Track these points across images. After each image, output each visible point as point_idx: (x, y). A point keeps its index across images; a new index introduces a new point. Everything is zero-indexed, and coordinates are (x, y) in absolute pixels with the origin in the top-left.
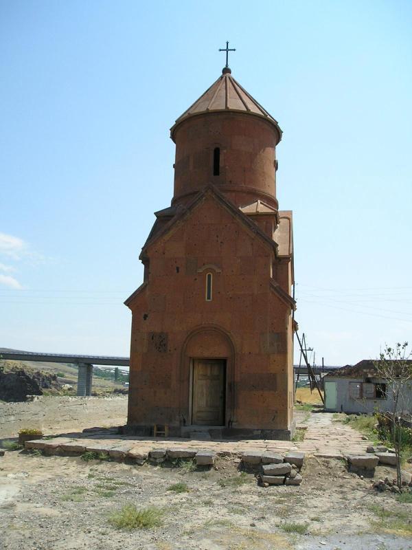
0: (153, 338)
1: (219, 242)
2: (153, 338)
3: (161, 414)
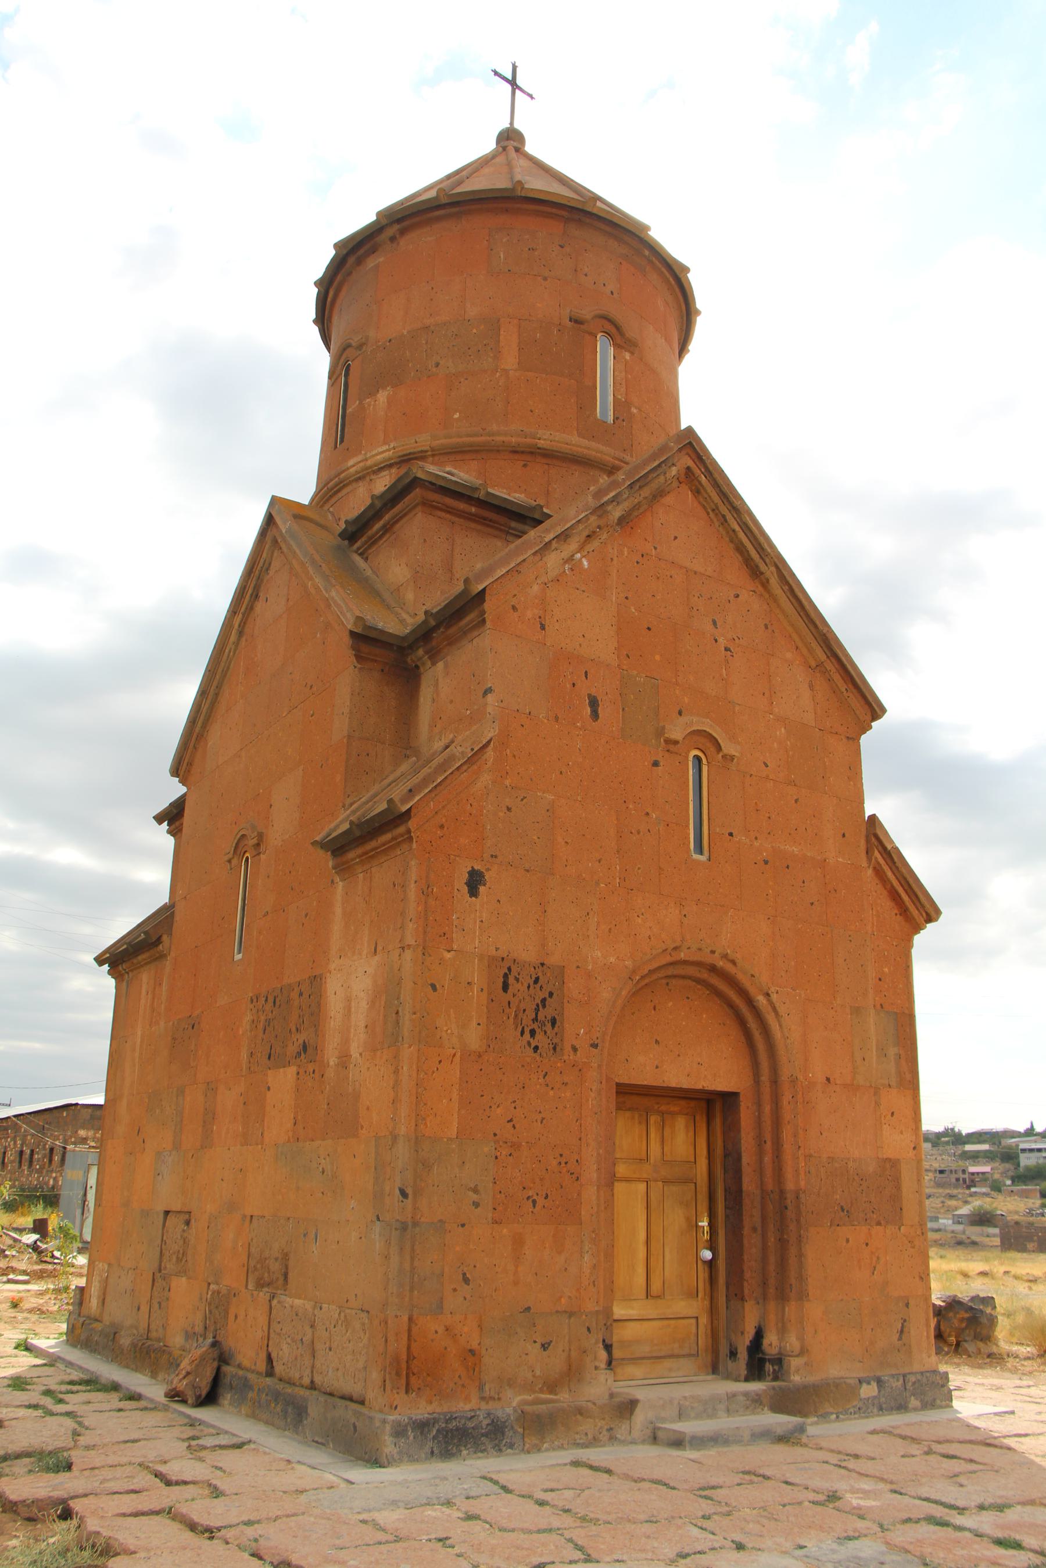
0: (505, 987)
2: (505, 987)
3: (544, 1347)
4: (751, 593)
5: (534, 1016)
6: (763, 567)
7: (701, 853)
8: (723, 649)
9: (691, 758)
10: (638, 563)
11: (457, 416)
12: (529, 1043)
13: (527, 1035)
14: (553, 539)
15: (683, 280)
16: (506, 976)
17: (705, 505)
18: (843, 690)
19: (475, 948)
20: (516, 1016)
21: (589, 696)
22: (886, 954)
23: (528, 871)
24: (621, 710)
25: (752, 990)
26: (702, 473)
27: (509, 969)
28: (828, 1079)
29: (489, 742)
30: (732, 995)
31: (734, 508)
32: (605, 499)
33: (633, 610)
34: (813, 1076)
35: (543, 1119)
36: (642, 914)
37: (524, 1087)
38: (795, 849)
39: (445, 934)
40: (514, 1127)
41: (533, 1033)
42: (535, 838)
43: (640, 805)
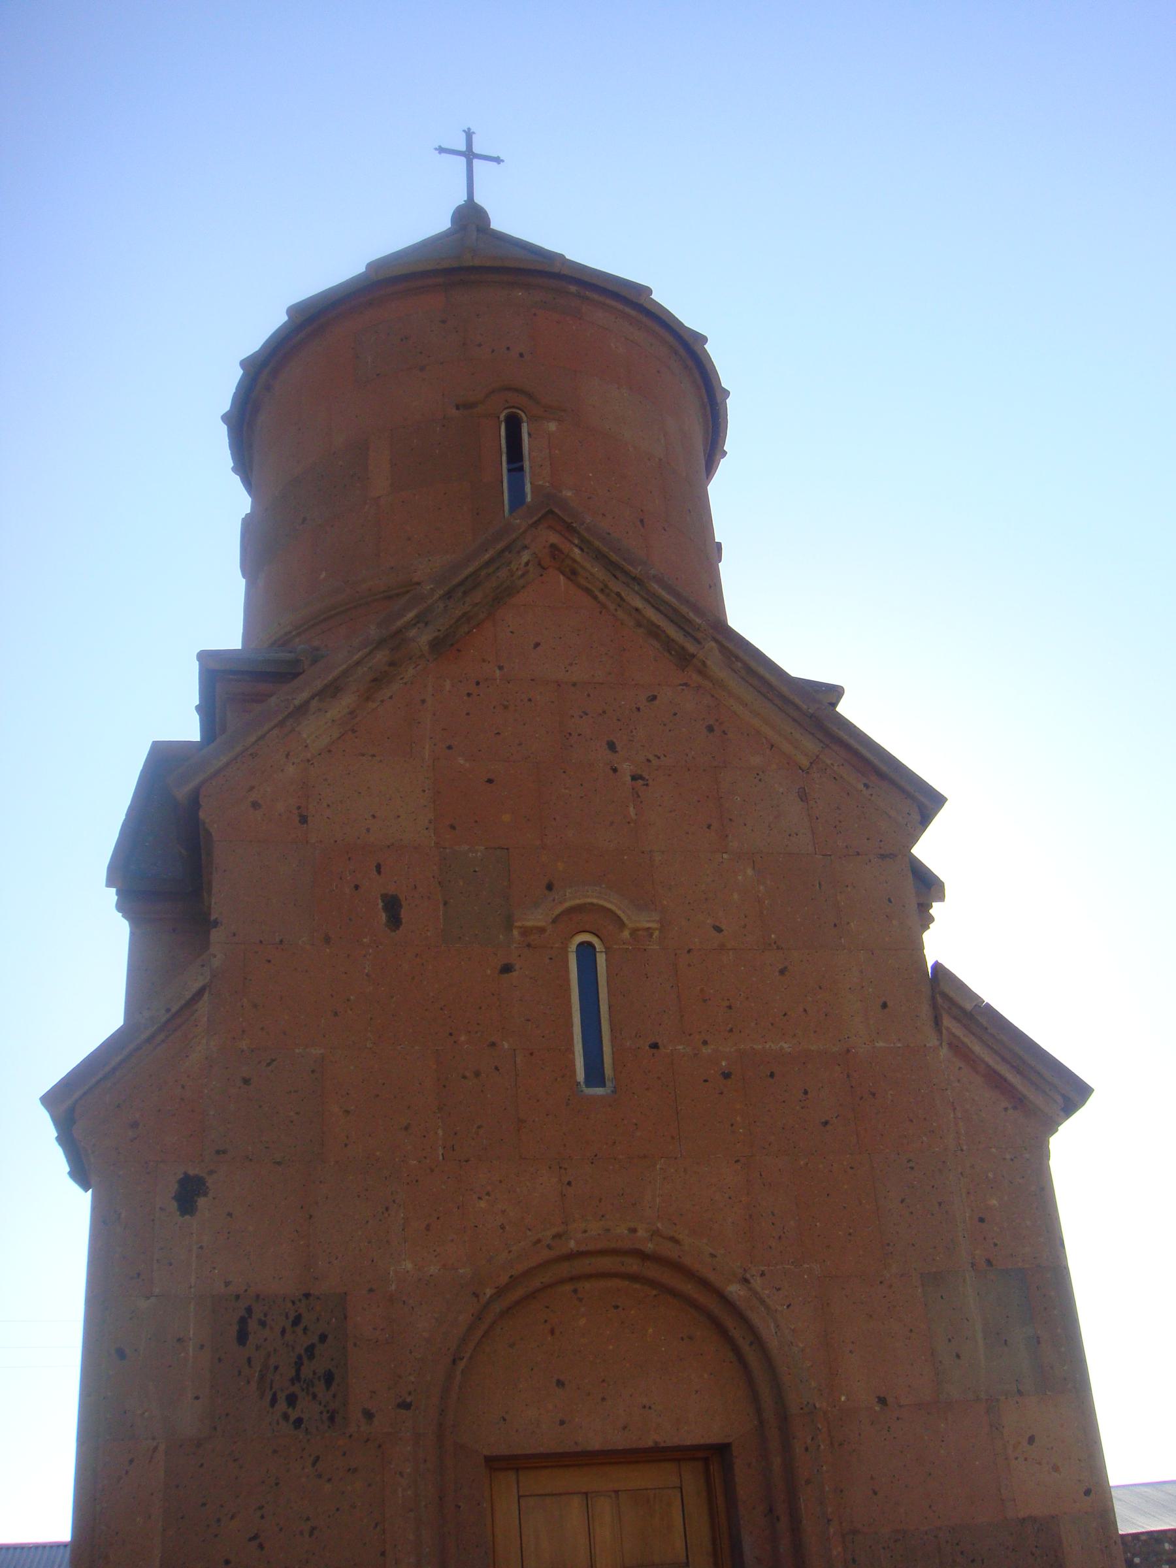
1: (626, 768)
2: (242, 1337)
4: (681, 687)
5: (293, 1373)
6: (691, 648)
7: (603, 1085)
8: (630, 778)
9: (573, 947)
10: (469, 695)
11: (323, 575)
12: (286, 1417)
13: (282, 1405)
14: (313, 697)
15: (649, 307)
16: (243, 1321)
17: (589, 586)
18: (861, 787)
19: (191, 1287)
20: (262, 1378)
21: (384, 897)
22: (990, 1175)
23: (279, 1163)
24: (441, 906)
25: (712, 1277)
26: (576, 546)
27: (249, 1310)
28: (882, 1401)
29: (200, 993)
30: (689, 1288)
31: (634, 579)
32: (399, 623)
33: (462, 762)
34: (848, 1399)
35: (313, 1529)
36: (488, 1194)
37: (277, 1484)
38: (785, 1046)
39: (139, 1274)
40: (261, 1546)
41: (292, 1400)
42: (292, 1114)
43: (479, 1034)
